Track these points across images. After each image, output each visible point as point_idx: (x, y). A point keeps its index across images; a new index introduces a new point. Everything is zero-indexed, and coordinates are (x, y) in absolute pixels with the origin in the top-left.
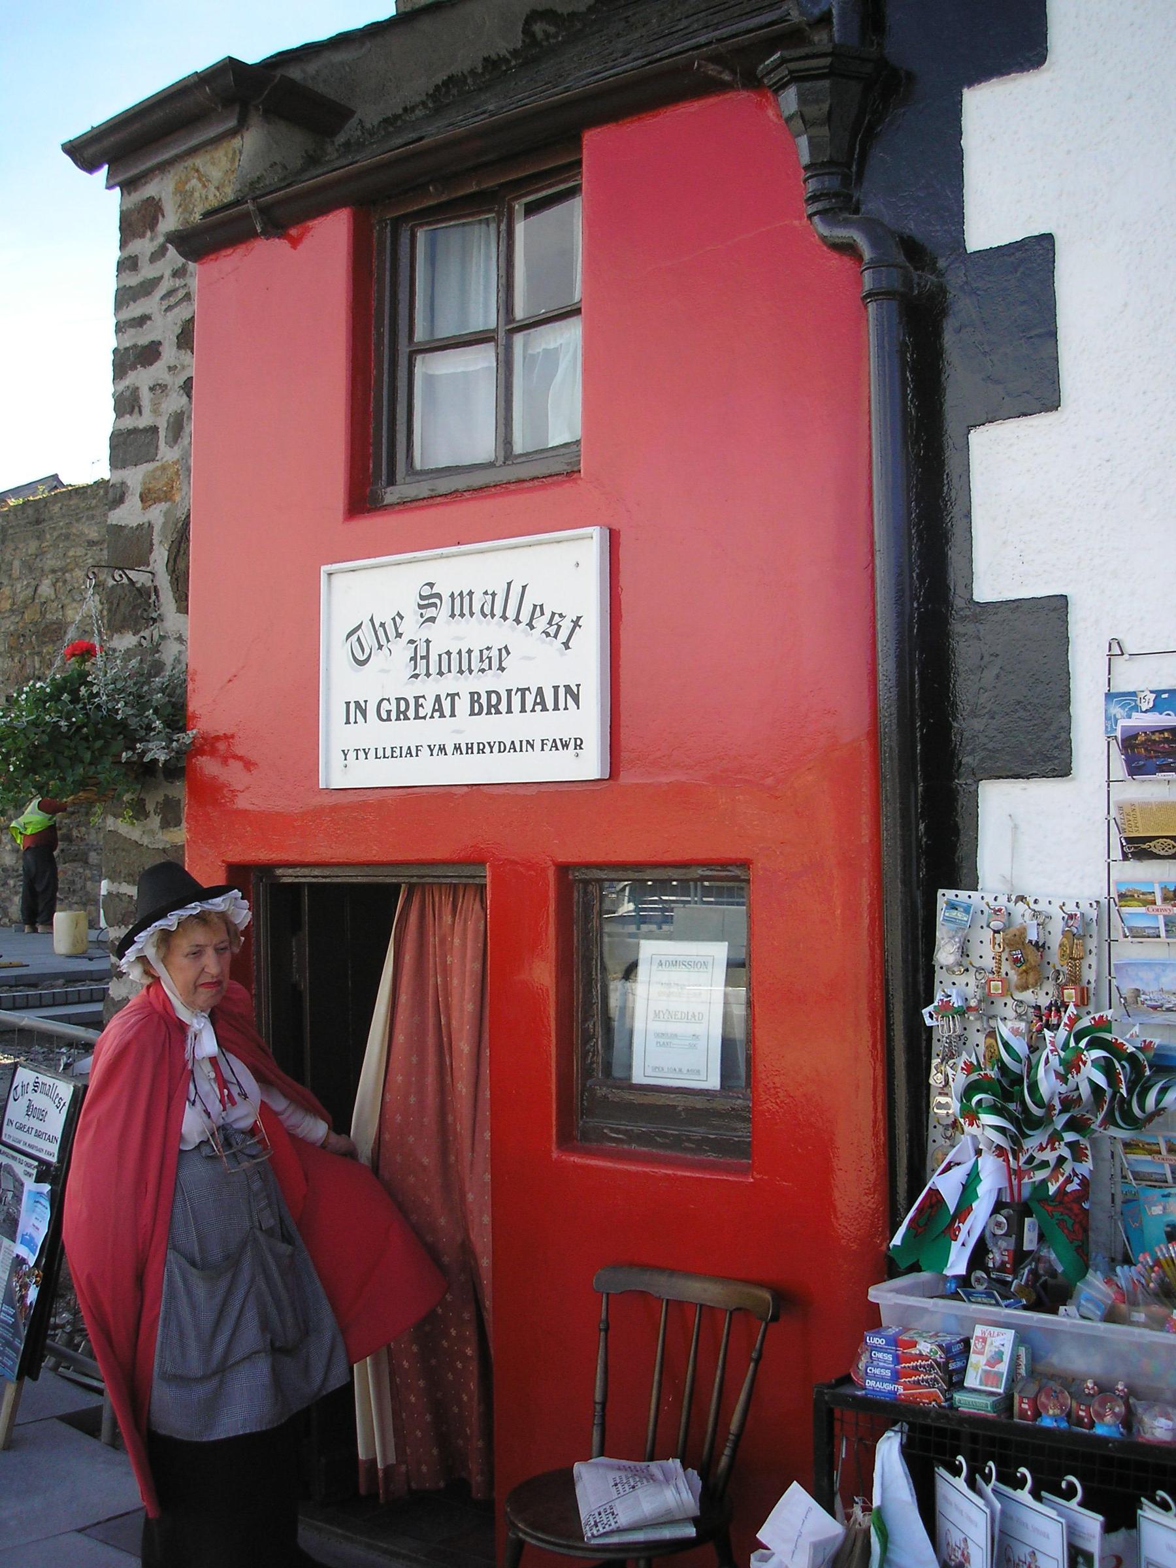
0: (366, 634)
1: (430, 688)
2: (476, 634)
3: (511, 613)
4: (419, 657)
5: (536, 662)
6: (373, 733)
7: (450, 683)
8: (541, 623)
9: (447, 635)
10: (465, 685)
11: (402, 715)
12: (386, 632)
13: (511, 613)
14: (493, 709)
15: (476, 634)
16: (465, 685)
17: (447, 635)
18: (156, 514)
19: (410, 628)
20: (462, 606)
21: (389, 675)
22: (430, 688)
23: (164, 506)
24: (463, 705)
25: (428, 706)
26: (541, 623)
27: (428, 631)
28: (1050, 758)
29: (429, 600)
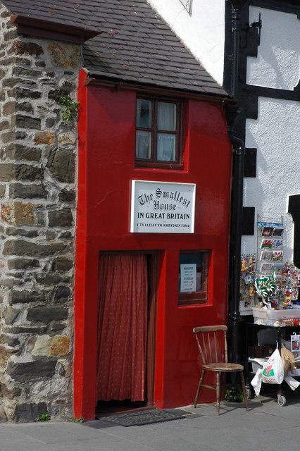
0: (143, 198)
1: (159, 212)
2: (169, 201)
3: (176, 198)
4: (156, 205)
5: (180, 209)
6: (143, 220)
7: (163, 211)
8: (182, 201)
9: (162, 201)
10: (166, 212)
11: (152, 217)
12: (149, 198)
13: (176, 198)
14: (172, 217)
15: (169, 201)
16: (166, 212)
17: (162, 201)
18: (41, 146)
19: (154, 197)
20: (166, 195)
21: (148, 208)
22: (159, 212)
23: (46, 145)
24: (166, 216)
25: (158, 215)
26: (182, 201)
27: (158, 200)
28: (251, 233)
29: (159, 192)
